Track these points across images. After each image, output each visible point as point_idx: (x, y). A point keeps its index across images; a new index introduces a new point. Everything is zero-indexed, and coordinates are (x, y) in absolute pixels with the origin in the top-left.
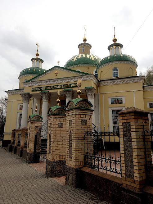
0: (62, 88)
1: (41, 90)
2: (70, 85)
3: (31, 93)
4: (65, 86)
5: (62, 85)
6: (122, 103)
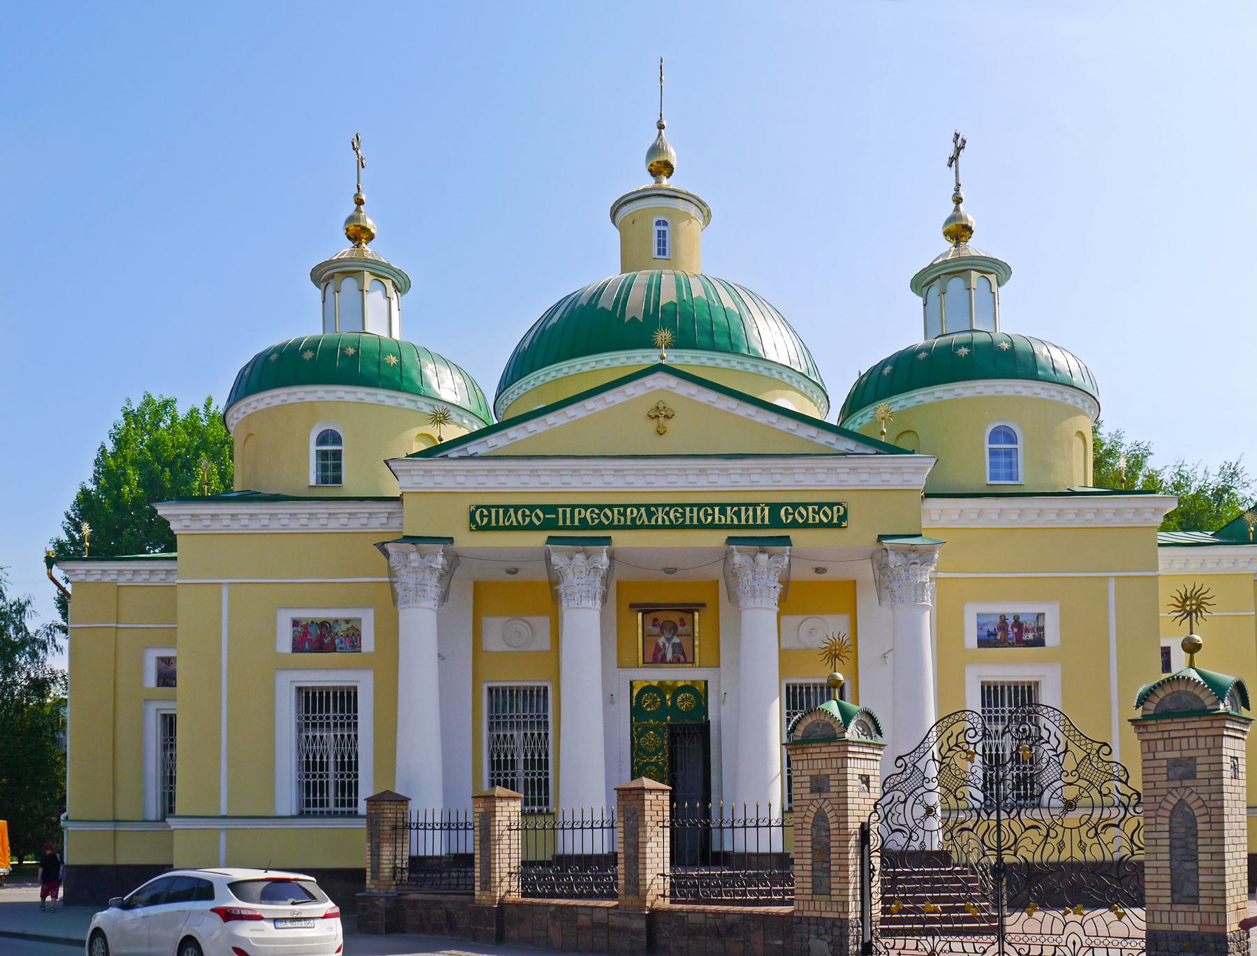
0: (712, 526)
1: (546, 525)
2: (775, 508)
3: (467, 540)
4: (738, 514)
5: (712, 506)
6: (1039, 642)
